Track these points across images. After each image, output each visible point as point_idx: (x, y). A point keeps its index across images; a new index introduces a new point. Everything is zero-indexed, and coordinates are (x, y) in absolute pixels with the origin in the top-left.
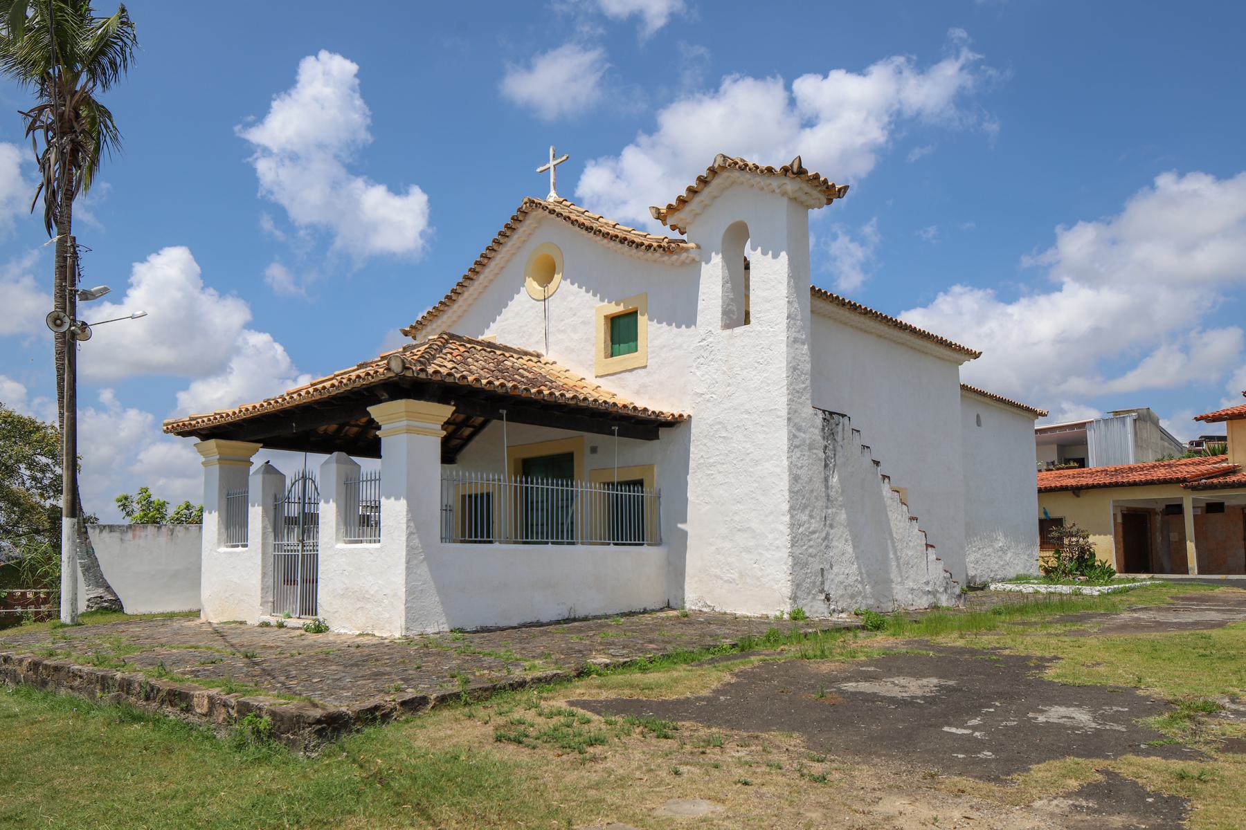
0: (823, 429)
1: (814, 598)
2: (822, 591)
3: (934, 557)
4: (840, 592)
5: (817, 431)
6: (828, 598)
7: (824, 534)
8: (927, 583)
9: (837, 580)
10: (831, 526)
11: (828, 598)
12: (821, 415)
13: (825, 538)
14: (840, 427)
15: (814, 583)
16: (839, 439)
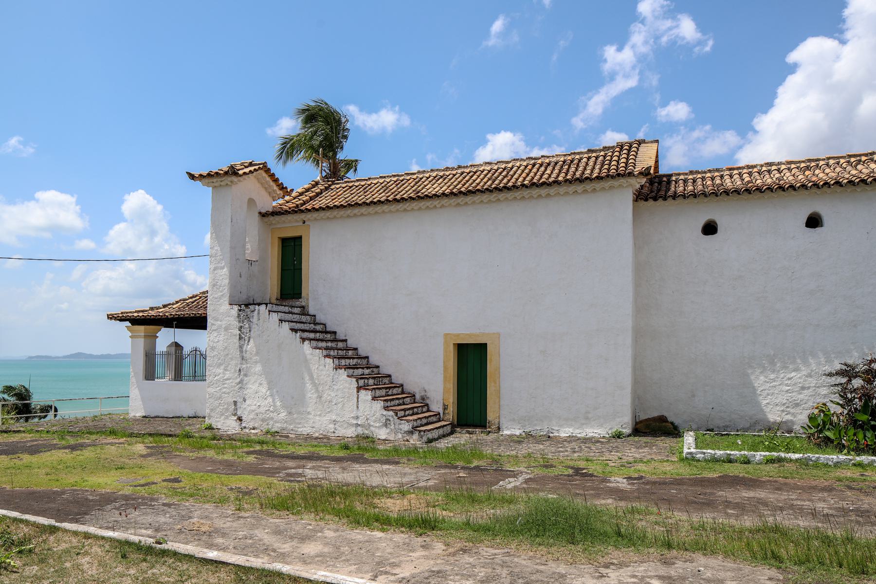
0: (239, 316)
1: (227, 417)
2: (235, 415)
3: (370, 397)
4: (251, 416)
5: (232, 319)
6: (240, 419)
7: (238, 380)
8: (357, 418)
9: (249, 409)
10: (246, 375)
11: (240, 419)
12: (236, 308)
13: (241, 382)
14: (256, 312)
15: (227, 409)
16: (255, 320)
